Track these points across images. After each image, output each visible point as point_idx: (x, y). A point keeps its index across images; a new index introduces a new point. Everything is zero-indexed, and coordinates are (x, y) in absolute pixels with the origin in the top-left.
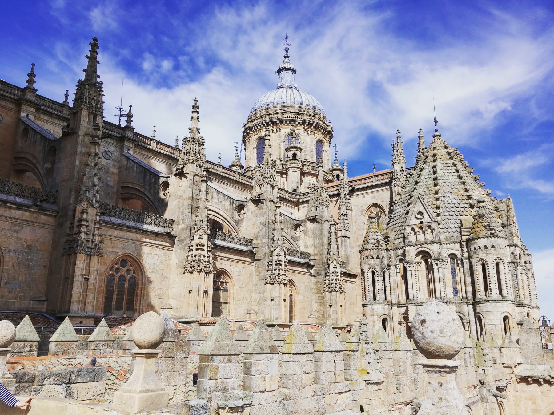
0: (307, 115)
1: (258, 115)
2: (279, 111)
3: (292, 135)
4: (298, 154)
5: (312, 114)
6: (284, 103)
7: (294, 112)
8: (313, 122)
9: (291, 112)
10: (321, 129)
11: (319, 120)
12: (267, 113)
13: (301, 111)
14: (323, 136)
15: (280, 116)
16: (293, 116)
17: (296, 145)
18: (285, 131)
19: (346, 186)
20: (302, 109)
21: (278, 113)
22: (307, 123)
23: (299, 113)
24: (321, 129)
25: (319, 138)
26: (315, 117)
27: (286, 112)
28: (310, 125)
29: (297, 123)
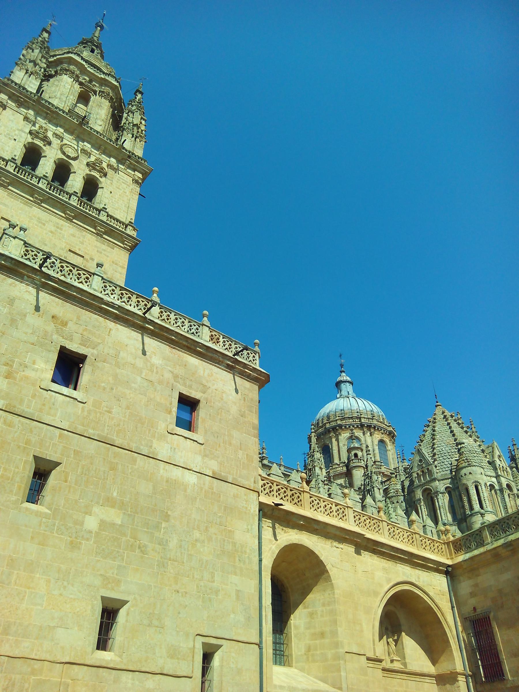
0: (365, 418)
1: (321, 425)
2: (338, 418)
3: (352, 438)
4: (360, 454)
5: (370, 417)
6: (341, 410)
7: (352, 417)
8: (371, 423)
9: (349, 417)
10: (381, 429)
11: (378, 421)
12: (327, 421)
13: (358, 415)
14: (385, 436)
15: (339, 422)
16: (351, 420)
17: (356, 445)
18: (345, 435)
19: (402, 474)
20: (359, 414)
21: (336, 420)
22: (366, 425)
23: (356, 417)
24: (381, 429)
25: (380, 438)
26: (372, 419)
27: (344, 418)
28: (369, 427)
29: (355, 426)
